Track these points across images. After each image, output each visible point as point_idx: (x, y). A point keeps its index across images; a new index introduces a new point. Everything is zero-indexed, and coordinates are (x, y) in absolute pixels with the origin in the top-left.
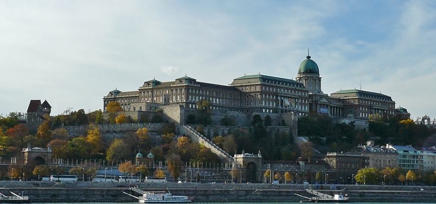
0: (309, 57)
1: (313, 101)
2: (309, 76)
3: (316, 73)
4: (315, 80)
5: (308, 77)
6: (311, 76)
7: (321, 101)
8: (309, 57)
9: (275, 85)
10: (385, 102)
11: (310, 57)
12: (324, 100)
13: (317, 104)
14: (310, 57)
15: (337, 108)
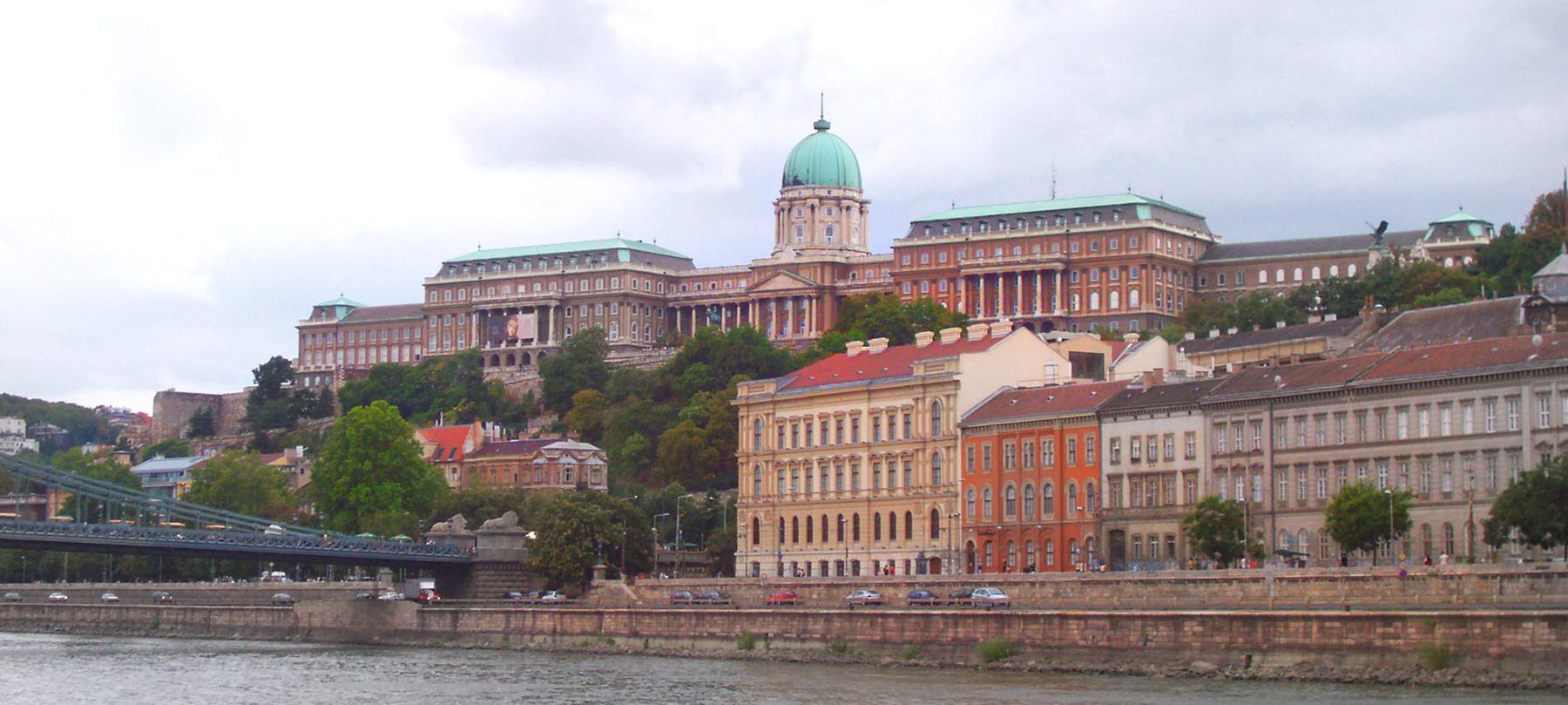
0: (821, 127)
3: (797, 182)
8: (821, 127)
10: (1068, 235)
12: (782, 283)
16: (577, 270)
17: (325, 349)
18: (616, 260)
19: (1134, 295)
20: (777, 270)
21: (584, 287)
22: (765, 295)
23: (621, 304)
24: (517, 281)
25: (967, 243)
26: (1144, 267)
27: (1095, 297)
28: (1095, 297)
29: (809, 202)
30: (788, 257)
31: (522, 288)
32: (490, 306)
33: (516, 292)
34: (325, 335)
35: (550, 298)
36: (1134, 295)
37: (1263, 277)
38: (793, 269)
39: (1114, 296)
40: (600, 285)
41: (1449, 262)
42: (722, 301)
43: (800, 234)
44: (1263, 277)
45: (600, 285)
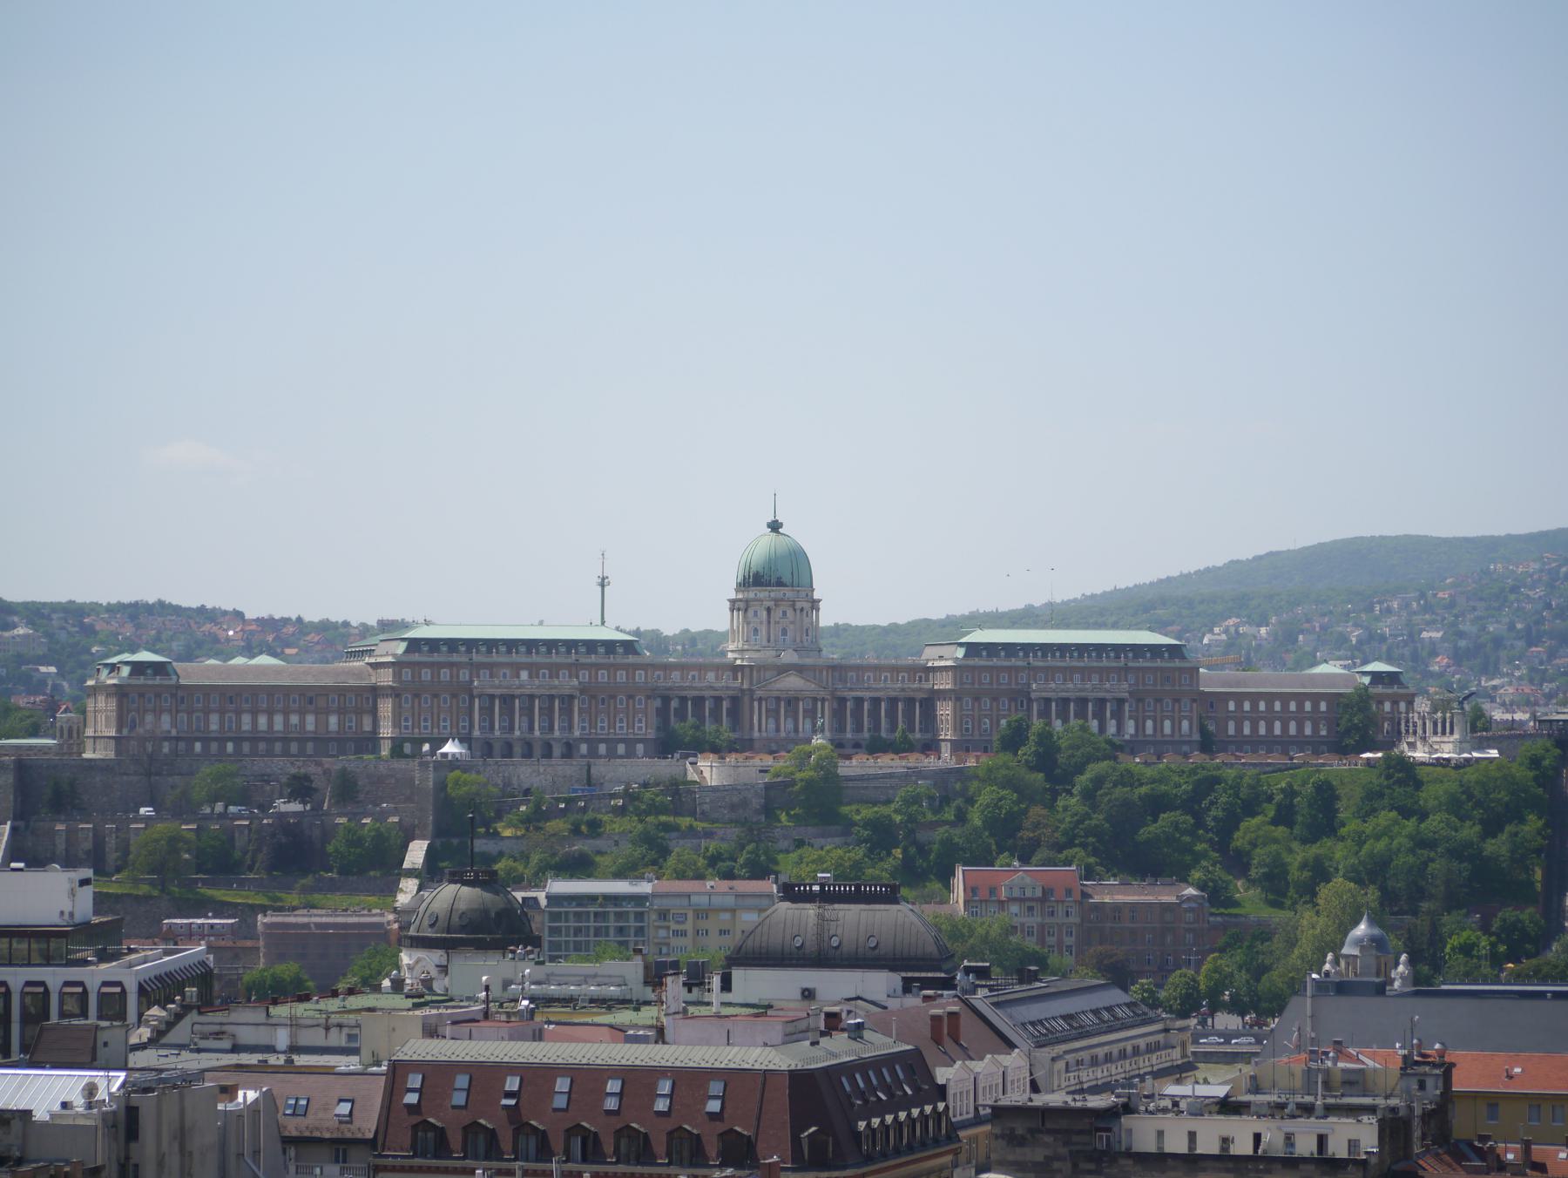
0: (775, 526)
1: (742, 691)
2: (751, 595)
3: (780, 583)
4: (769, 610)
5: (747, 601)
6: (761, 595)
7: (778, 686)
8: (775, 526)
9: (464, 659)
10: (1127, 669)
11: (781, 525)
12: (793, 682)
13: (752, 700)
14: (781, 525)
15: (893, 701)
16: (593, 658)
17: (158, 713)
18: (636, 653)
19: (1185, 724)
20: (783, 670)
21: (603, 676)
22: (776, 694)
23: (648, 697)
24: (517, 668)
25: (1029, 667)
26: (1194, 701)
27: (1149, 723)
28: (1149, 723)
29: (798, 605)
30: (789, 657)
31: (524, 675)
32: (498, 692)
33: (518, 676)
34: (158, 696)
35: (573, 687)
36: (1185, 724)
37: (1232, 706)
38: (799, 669)
39: (1167, 724)
40: (621, 676)
41: (1387, 706)
42: (706, 693)
43: (784, 632)
44: (1232, 706)
45: (621, 676)
